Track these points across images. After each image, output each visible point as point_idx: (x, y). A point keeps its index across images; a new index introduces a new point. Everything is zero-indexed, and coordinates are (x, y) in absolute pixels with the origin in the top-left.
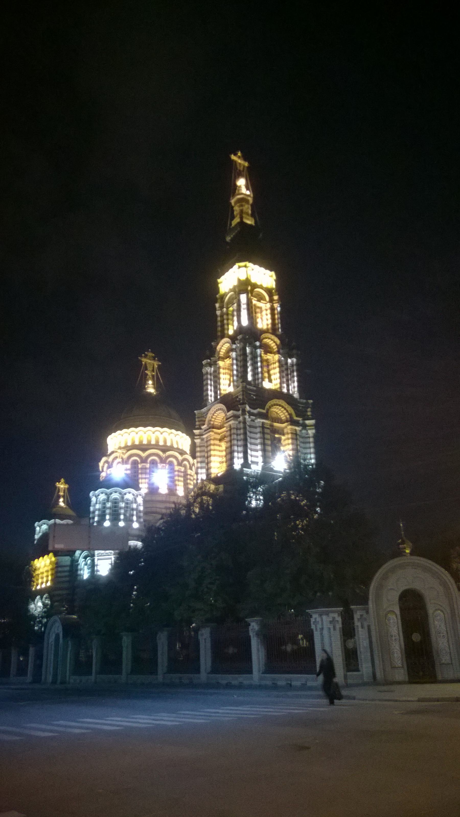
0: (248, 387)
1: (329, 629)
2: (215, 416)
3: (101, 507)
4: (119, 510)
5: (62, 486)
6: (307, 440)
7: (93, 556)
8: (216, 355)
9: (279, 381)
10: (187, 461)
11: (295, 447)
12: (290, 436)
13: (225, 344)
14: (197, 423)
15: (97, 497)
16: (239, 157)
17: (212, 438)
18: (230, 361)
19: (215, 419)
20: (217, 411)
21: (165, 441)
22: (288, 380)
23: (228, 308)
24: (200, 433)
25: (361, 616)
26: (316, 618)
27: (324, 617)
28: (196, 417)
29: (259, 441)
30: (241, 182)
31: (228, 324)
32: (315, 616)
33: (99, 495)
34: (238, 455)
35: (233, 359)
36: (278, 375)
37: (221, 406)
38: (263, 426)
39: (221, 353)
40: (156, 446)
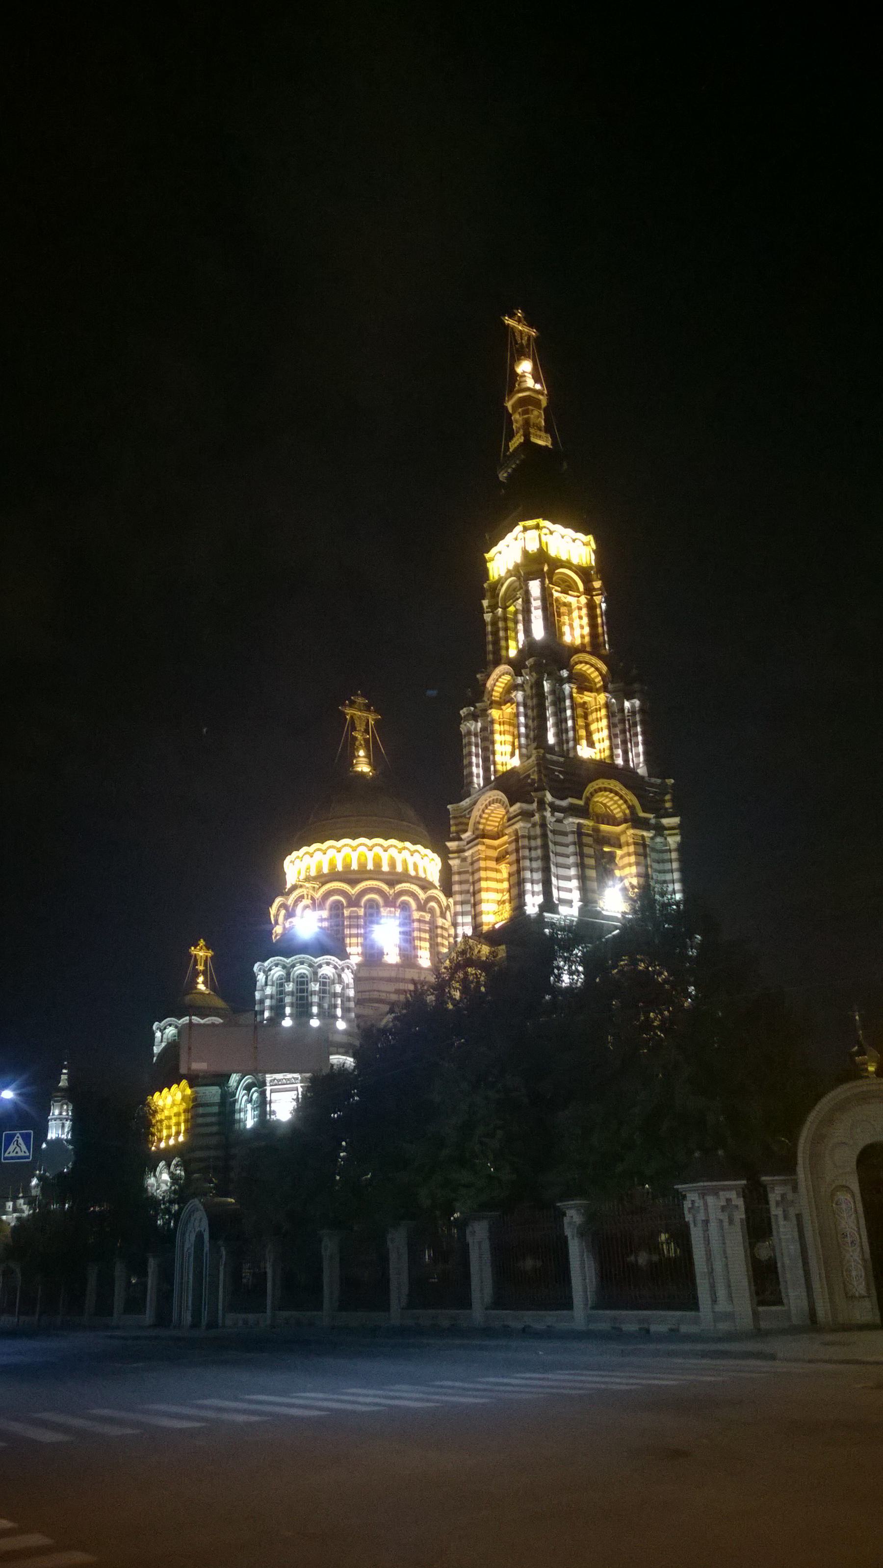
0: (548, 756)
1: (721, 1221)
2: (487, 813)
3: (274, 993)
4: (310, 998)
5: (201, 952)
6: (666, 856)
7: (264, 1084)
8: (485, 699)
9: (607, 743)
10: (436, 903)
11: (642, 870)
12: (632, 849)
13: (503, 677)
14: (453, 829)
15: (267, 972)
16: (519, 321)
17: (482, 856)
18: (512, 709)
19: (487, 819)
20: (490, 805)
21: (393, 864)
22: (624, 742)
23: (505, 608)
24: (458, 846)
25: (783, 1196)
26: (693, 1202)
27: (710, 1200)
28: (451, 816)
29: (572, 860)
30: (525, 367)
31: (507, 639)
32: (692, 1196)
33: (270, 970)
34: (533, 887)
35: (518, 705)
36: (606, 733)
37: (498, 795)
38: (579, 832)
40: (376, 873)
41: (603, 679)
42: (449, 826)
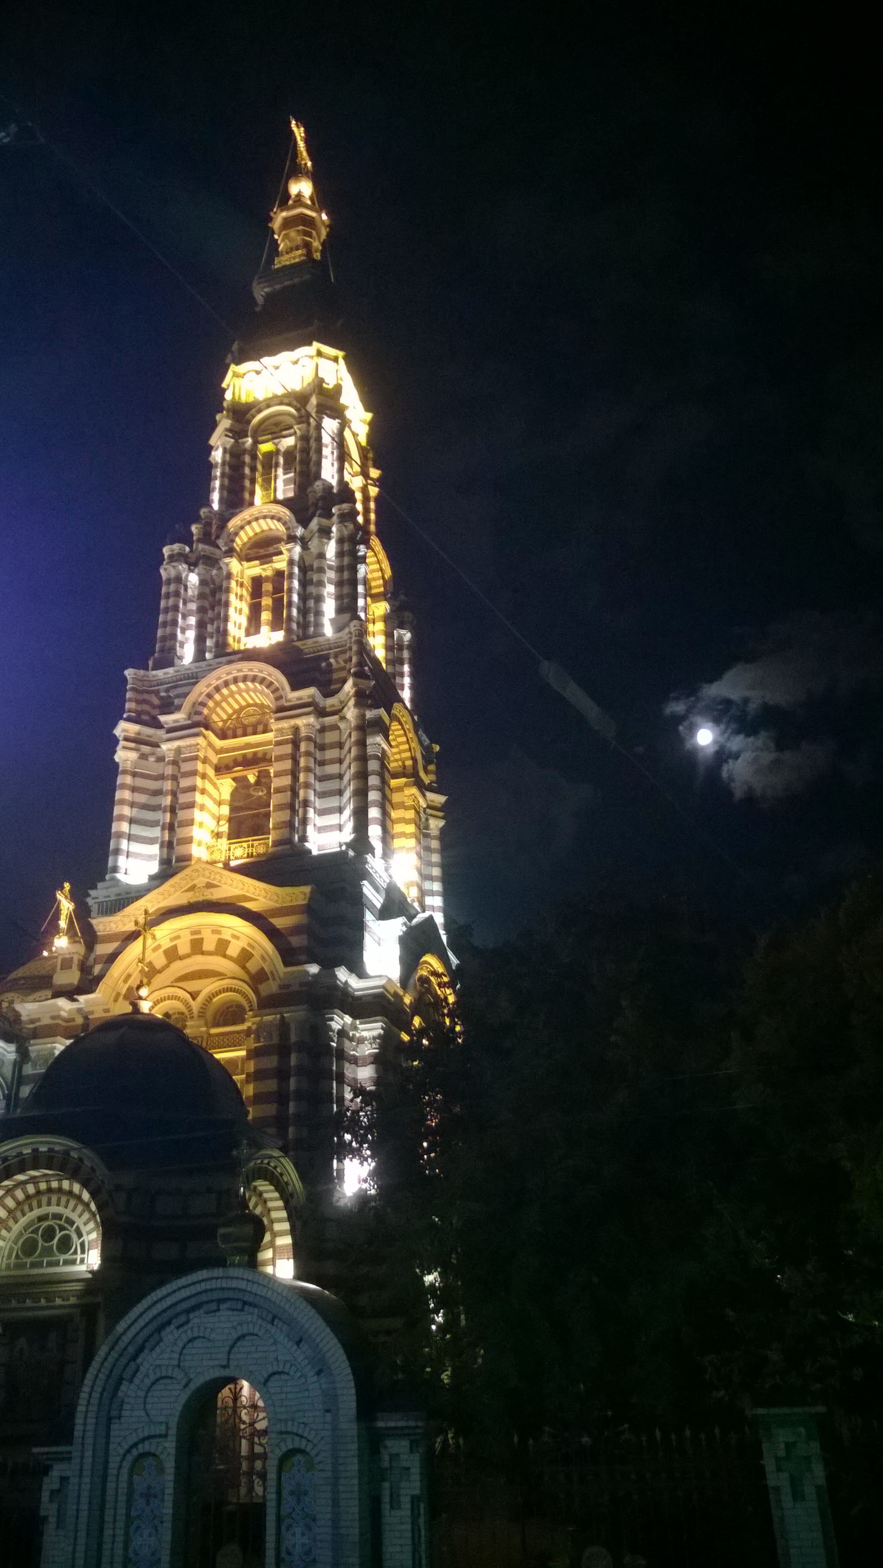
13: (269, 520)
17: (201, 754)
23: (256, 443)
24: (139, 734)
28: (128, 687)
31: (253, 481)
41: (385, 584)
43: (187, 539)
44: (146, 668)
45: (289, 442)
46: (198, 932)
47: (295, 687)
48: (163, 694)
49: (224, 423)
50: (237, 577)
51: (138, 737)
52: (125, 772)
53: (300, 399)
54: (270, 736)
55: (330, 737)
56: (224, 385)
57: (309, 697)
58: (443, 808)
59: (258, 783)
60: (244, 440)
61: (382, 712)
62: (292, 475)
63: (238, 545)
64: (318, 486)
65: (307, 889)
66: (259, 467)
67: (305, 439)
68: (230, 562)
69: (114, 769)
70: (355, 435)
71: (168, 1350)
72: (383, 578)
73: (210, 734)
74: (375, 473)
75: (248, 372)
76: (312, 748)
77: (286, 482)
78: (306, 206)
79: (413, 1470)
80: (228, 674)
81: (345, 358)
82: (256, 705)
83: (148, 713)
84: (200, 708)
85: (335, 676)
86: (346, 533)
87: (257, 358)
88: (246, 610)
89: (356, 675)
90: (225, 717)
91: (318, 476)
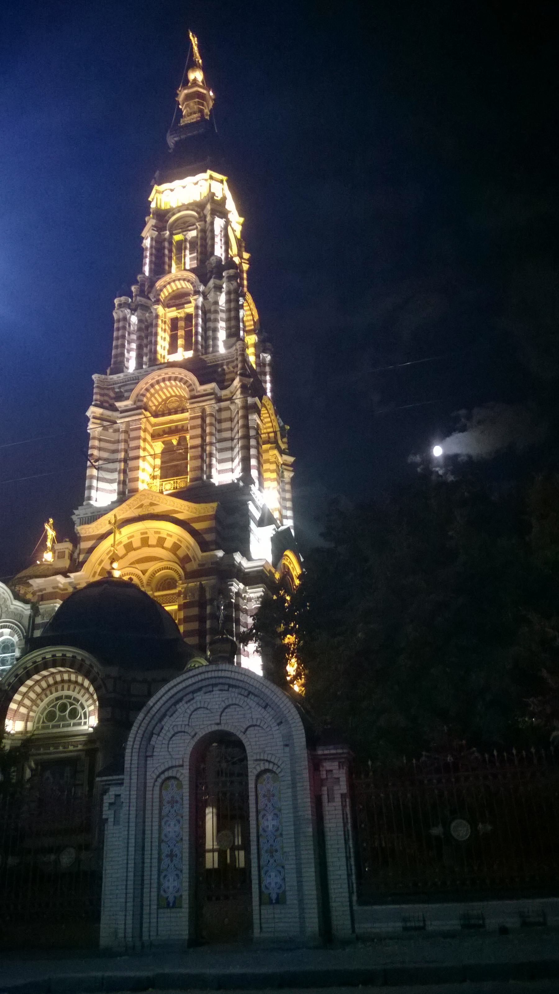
13: (182, 282)
17: (143, 426)
19: (152, 395)
23: (172, 234)
24: (102, 414)
31: (170, 258)
39: (162, 294)
41: (255, 323)
42: (92, 394)
43: (130, 295)
44: (106, 374)
45: (193, 234)
46: (146, 533)
47: (202, 383)
48: (117, 390)
49: (151, 222)
50: (162, 317)
51: (102, 416)
52: (94, 438)
53: (199, 207)
54: (186, 415)
55: (225, 415)
56: (150, 199)
57: (211, 389)
58: (292, 465)
59: (179, 443)
60: (164, 232)
61: (257, 399)
62: (195, 255)
63: (162, 298)
64: (213, 260)
65: (215, 505)
66: (174, 250)
67: (203, 231)
68: (157, 308)
69: (87, 437)
70: (234, 231)
71: (182, 716)
72: (253, 320)
73: (148, 414)
74: (246, 255)
75: (166, 190)
76: (213, 421)
77: (191, 259)
78: (200, 86)
79: (341, 779)
80: (159, 376)
81: (227, 181)
82: (176, 396)
83: (107, 402)
84: (141, 398)
85: (227, 377)
86: (232, 288)
87: (171, 181)
88: (168, 339)
89: (241, 375)
90: (157, 404)
91: (212, 253)
